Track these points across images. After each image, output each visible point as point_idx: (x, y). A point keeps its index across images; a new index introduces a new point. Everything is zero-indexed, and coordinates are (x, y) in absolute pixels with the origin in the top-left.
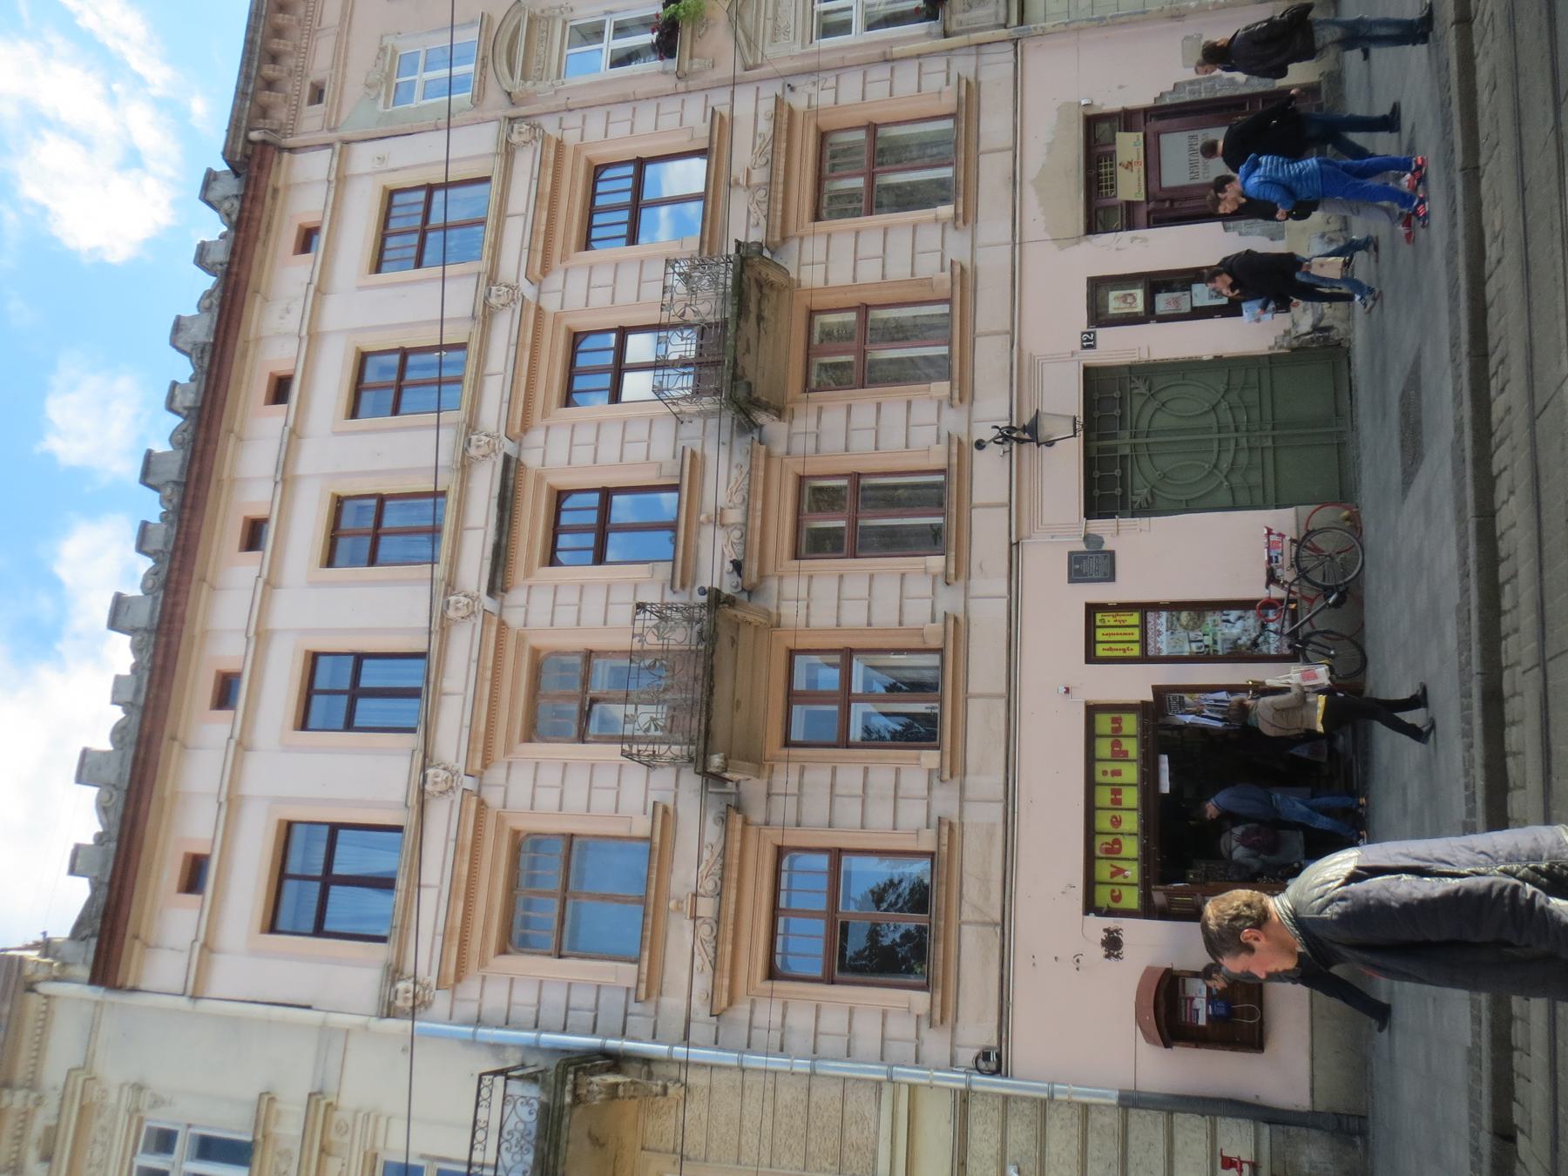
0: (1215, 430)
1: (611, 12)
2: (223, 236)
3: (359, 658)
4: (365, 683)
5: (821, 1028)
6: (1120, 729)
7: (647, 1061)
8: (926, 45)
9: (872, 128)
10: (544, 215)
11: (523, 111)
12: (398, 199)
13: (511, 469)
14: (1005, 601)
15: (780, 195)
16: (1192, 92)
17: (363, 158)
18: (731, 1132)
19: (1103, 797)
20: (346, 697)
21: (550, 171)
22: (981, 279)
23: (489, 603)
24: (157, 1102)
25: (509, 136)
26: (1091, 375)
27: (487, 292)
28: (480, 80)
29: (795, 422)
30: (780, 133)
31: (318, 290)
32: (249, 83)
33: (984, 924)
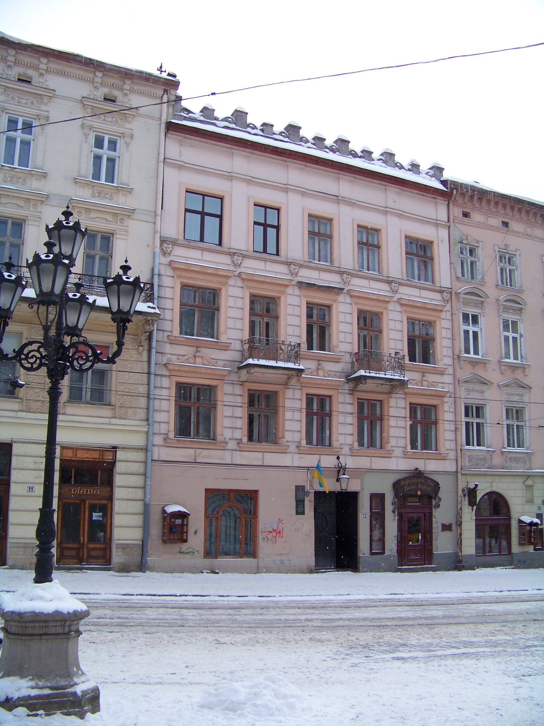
3: (277, 228)
5: (162, 401)
8: (459, 443)
9: (436, 423)
17: (443, 233)
21: (434, 308)
33: (195, 456)
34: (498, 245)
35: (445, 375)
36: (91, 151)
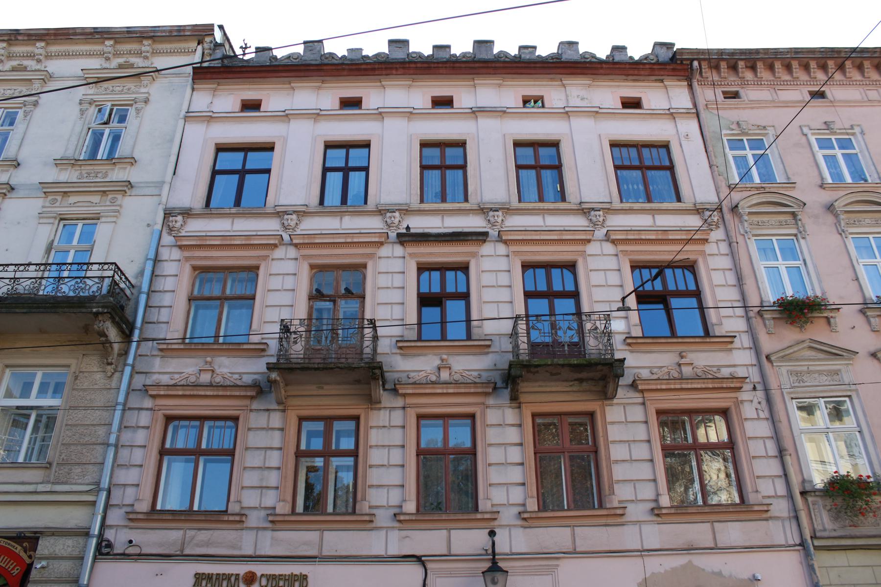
1: (805, 264)
2: (631, 58)
3: (366, 169)
4: (352, 175)
7: (125, 353)
10: (653, 237)
11: (728, 216)
12: (663, 151)
13: (481, 237)
14: (383, 553)
15: (672, 387)
17: (690, 126)
18: (86, 402)
20: (344, 165)
22: (614, 529)
23: (393, 235)
24: (138, 111)
25: (708, 209)
27: (598, 209)
28: (747, 188)
29: (510, 410)
30: (719, 383)
31: (597, 112)
32: (728, 55)
33: (183, 544)
34: (805, 126)
35: (734, 351)
36: (89, 129)
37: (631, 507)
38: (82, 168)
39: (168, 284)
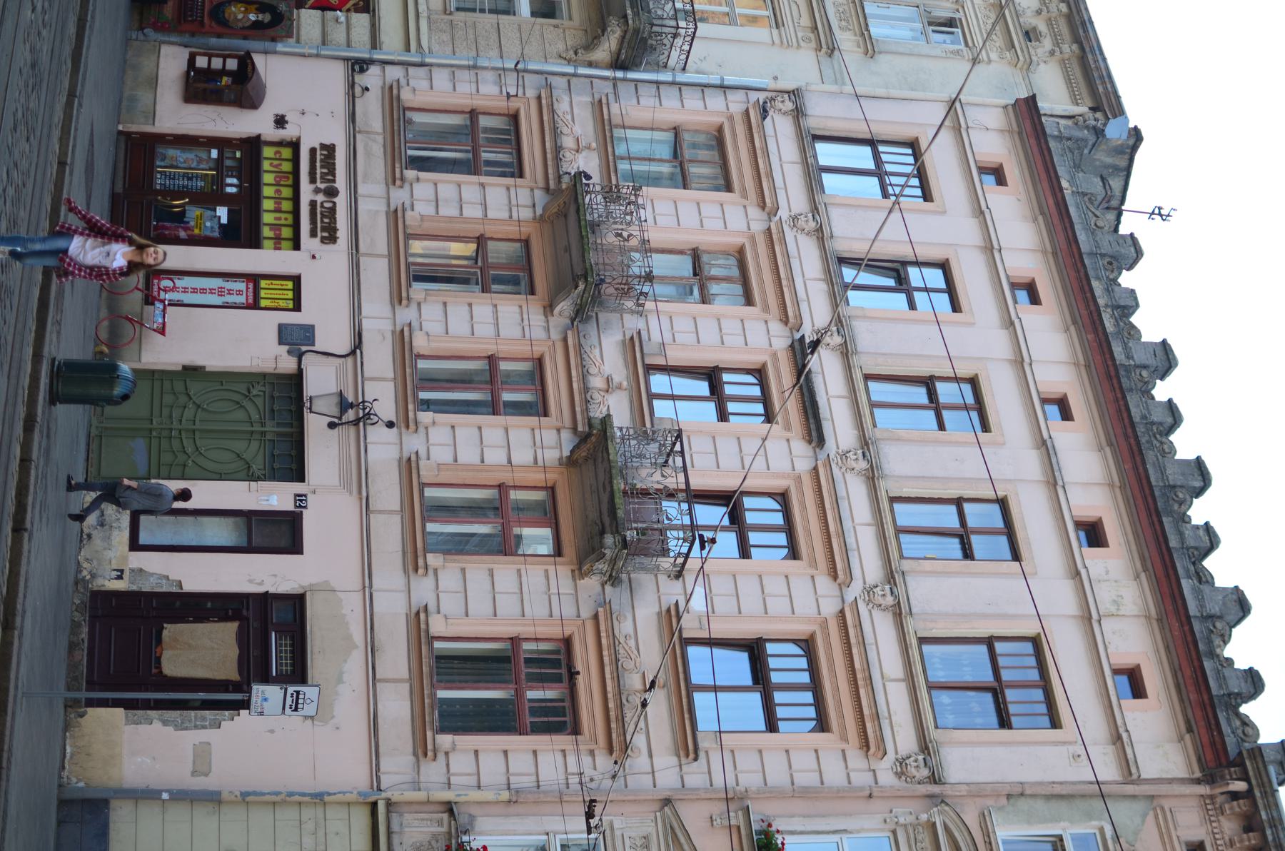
0: (197, 433)
6: (275, 243)
10: (857, 665)
15: (605, 653)
16: (204, 719)
19: (286, 205)
21: (866, 711)
26: (300, 476)
28: (989, 837)
32: (1274, 839)
33: (367, 132)
37: (428, 582)
38: (851, 5)
39: (693, 101)
